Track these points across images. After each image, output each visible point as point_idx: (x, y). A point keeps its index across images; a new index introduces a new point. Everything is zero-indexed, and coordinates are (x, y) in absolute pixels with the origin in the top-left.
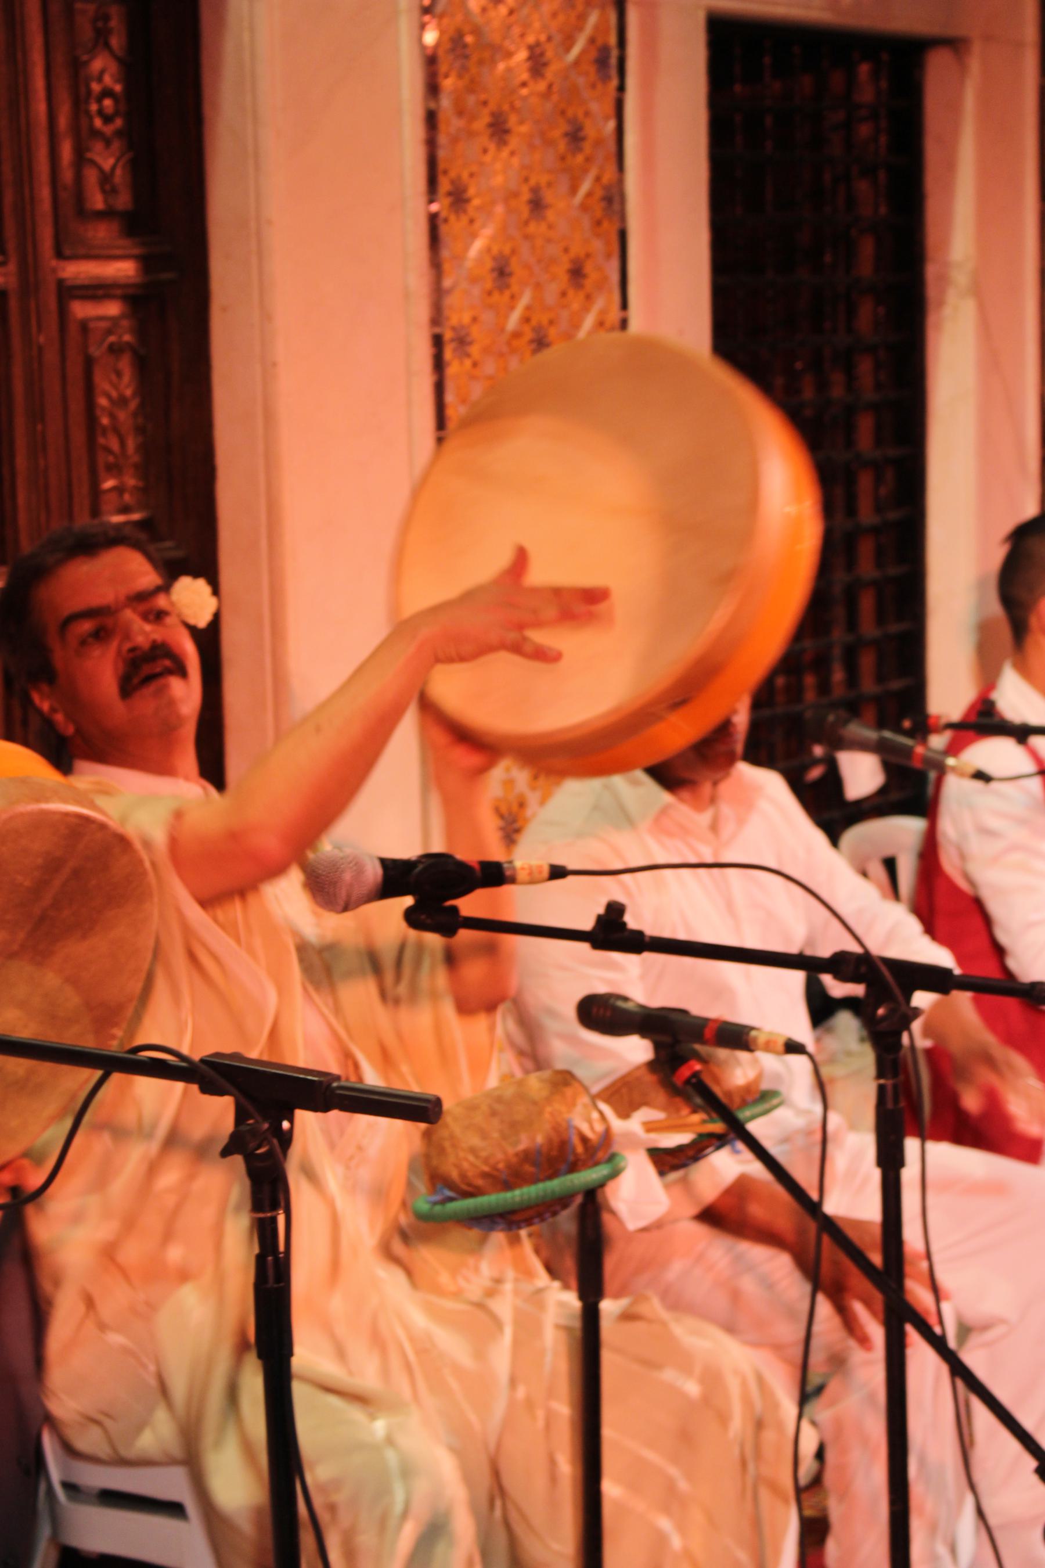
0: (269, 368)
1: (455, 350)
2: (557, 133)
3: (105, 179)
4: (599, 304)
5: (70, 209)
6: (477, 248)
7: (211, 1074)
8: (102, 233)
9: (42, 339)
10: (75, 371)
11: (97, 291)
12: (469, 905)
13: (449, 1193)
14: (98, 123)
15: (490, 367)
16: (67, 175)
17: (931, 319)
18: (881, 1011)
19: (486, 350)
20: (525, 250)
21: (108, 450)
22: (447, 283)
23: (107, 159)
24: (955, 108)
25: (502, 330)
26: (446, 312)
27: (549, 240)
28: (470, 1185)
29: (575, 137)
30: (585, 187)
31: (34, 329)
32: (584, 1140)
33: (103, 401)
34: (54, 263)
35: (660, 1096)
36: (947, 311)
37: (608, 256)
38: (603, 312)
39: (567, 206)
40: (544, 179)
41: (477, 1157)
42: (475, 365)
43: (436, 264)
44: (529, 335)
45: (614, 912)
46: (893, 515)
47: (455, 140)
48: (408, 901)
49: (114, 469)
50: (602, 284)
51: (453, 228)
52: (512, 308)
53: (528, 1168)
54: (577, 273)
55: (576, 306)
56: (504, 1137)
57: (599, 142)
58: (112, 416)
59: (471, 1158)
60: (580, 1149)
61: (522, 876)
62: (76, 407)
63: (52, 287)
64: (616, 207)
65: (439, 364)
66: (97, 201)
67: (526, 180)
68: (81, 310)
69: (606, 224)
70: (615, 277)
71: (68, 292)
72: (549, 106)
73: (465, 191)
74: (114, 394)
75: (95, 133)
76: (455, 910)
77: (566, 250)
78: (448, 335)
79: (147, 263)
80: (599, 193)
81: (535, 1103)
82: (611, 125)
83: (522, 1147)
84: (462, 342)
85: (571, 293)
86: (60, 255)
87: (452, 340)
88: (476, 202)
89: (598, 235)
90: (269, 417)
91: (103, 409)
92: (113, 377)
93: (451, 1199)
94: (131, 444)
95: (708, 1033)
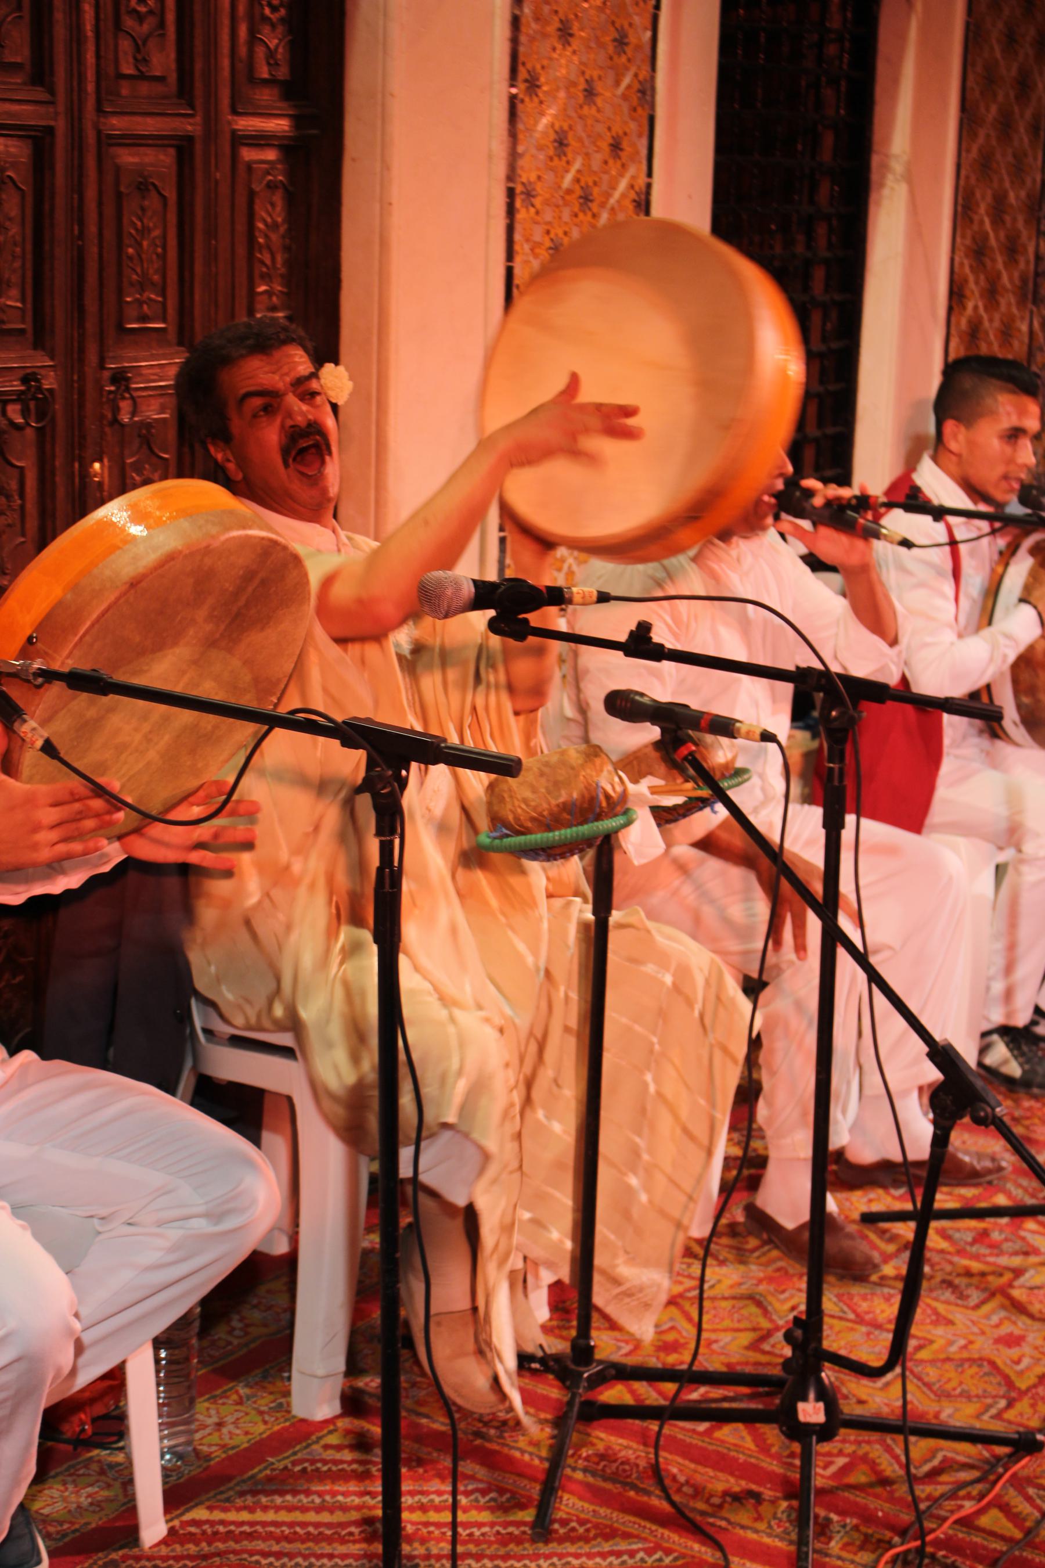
0: (386, 205)
1: (523, 201)
2: (607, 39)
3: (271, 54)
4: (632, 171)
5: (245, 77)
6: (544, 122)
7: (351, 733)
8: (266, 96)
9: (218, 175)
10: (241, 201)
11: (260, 140)
12: (534, 618)
13: (505, 831)
14: (267, 11)
15: (548, 215)
16: (243, 51)
17: (873, 197)
18: (834, 713)
19: (546, 203)
21: (263, 263)
22: (520, 149)
23: (273, 39)
24: (902, 37)
25: (560, 187)
26: (519, 171)
27: (597, 121)
28: (521, 826)
29: (621, 42)
30: (626, 81)
31: (213, 169)
32: (608, 797)
35: (662, 768)
36: (886, 192)
37: (640, 136)
38: (633, 178)
39: (613, 95)
40: (595, 74)
41: (528, 805)
42: (537, 213)
43: (513, 135)
44: (579, 192)
45: (643, 630)
46: (835, 345)
47: (532, 39)
48: (491, 613)
49: (266, 278)
50: (634, 157)
51: (528, 107)
52: (567, 171)
53: (565, 816)
54: (616, 147)
55: (614, 173)
56: (549, 793)
57: (638, 47)
58: (266, 236)
59: (524, 806)
60: (604, 804)
61: (577, 598)
62: (241, 228)
63: (227, 136)
64: (648, 98)
65: (511, 211)
66: (264, 72)
67: (583, 73)
68: (248, 154)
69: (640, 110)
70: (644, 152)
71: (239, 140)
72: (603, 17)
73: (538, 79)
74: (269, 220)
75: (265, 19)
76: (526, 621)
77: (609, 129)
78: (519, 189)
79: (298, 121)
80: (637, 86)
81: (573, 768)
82: (648, 34)
83: (561, 800)
84: (529, 194)
85: (611, 162)
86: (235, 112)
87: (522, 193)
88: (545, 88)
89: (633, 119)
90: (384, 244)
91: (260, 230)
92: (269, 207)
93: (508, 836)
94: (279, 259)
95: (703, 723)
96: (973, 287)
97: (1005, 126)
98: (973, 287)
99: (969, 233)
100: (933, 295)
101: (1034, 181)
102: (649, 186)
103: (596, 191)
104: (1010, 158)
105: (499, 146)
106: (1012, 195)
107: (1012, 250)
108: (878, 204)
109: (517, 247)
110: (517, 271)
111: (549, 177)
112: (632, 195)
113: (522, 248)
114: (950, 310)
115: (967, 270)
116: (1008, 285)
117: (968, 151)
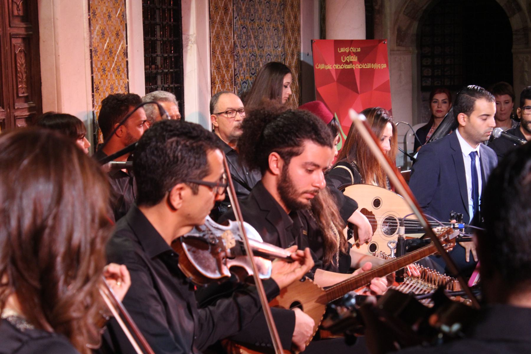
0: (57, 56)
3: (18, 6)
5: (11, 15)
6: (97, 28)
8: (17, 22)
11: (16, 36)
15: (101, 59)
19: (100, 54)
20: (107, 28)
22: (92, 36)
33: (18, 65)
34: (9, 29)
36: (189, 48)
38: (122, 45)
39: (116, 16)
43: (90, 31)
49: (21, 82)
51: (93, 22)
54: (117, 34)
62: (14, 66)
65: (91, 57)
66: (16, 13)
68: (14, 41)
70: (125, 36)
71: (12, 36)
78: (93, 50)
79: (27, 29)
84: (96, 51)
89: (121, 25)
90: (57, 69)
96: (218, 80)
97: (222, 23)
98: (218, 80)
99: (215, 61)
100: (207, 84)
101: (232, 42)
102: (127, 47)
103: (113, 50)
104: (224, 35)
105: (86, 35)
106: (226, 47)
107: (227, 67)
108: (187, 52)
109: (94, 69)
110: (94, 77)
111: (101, 45)
112: (123, 51)
113: (95, 69)
114: (212, 88)
115: (215, 74)
116: (228, 80)
117: (212, 33)
